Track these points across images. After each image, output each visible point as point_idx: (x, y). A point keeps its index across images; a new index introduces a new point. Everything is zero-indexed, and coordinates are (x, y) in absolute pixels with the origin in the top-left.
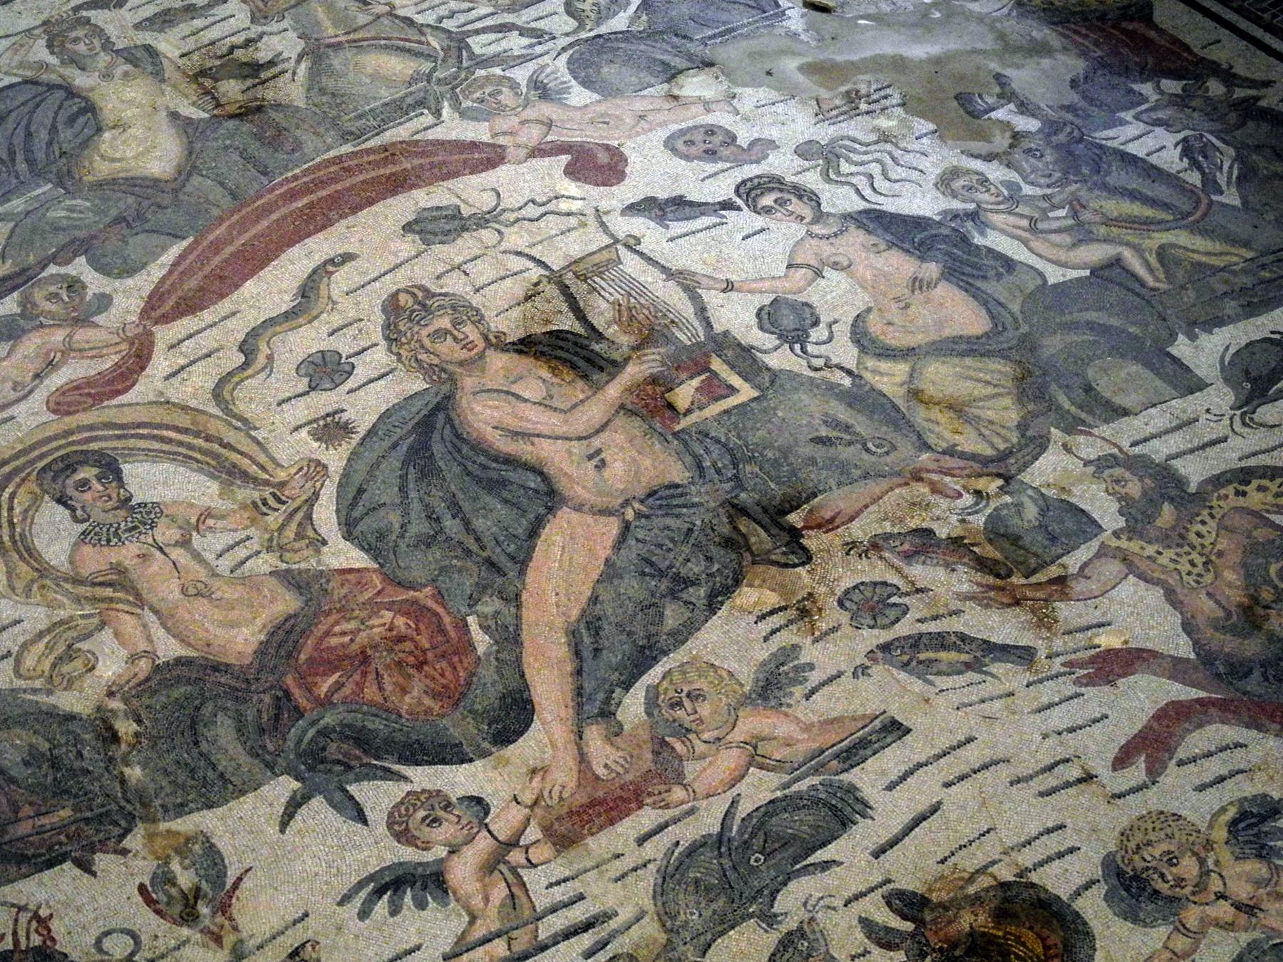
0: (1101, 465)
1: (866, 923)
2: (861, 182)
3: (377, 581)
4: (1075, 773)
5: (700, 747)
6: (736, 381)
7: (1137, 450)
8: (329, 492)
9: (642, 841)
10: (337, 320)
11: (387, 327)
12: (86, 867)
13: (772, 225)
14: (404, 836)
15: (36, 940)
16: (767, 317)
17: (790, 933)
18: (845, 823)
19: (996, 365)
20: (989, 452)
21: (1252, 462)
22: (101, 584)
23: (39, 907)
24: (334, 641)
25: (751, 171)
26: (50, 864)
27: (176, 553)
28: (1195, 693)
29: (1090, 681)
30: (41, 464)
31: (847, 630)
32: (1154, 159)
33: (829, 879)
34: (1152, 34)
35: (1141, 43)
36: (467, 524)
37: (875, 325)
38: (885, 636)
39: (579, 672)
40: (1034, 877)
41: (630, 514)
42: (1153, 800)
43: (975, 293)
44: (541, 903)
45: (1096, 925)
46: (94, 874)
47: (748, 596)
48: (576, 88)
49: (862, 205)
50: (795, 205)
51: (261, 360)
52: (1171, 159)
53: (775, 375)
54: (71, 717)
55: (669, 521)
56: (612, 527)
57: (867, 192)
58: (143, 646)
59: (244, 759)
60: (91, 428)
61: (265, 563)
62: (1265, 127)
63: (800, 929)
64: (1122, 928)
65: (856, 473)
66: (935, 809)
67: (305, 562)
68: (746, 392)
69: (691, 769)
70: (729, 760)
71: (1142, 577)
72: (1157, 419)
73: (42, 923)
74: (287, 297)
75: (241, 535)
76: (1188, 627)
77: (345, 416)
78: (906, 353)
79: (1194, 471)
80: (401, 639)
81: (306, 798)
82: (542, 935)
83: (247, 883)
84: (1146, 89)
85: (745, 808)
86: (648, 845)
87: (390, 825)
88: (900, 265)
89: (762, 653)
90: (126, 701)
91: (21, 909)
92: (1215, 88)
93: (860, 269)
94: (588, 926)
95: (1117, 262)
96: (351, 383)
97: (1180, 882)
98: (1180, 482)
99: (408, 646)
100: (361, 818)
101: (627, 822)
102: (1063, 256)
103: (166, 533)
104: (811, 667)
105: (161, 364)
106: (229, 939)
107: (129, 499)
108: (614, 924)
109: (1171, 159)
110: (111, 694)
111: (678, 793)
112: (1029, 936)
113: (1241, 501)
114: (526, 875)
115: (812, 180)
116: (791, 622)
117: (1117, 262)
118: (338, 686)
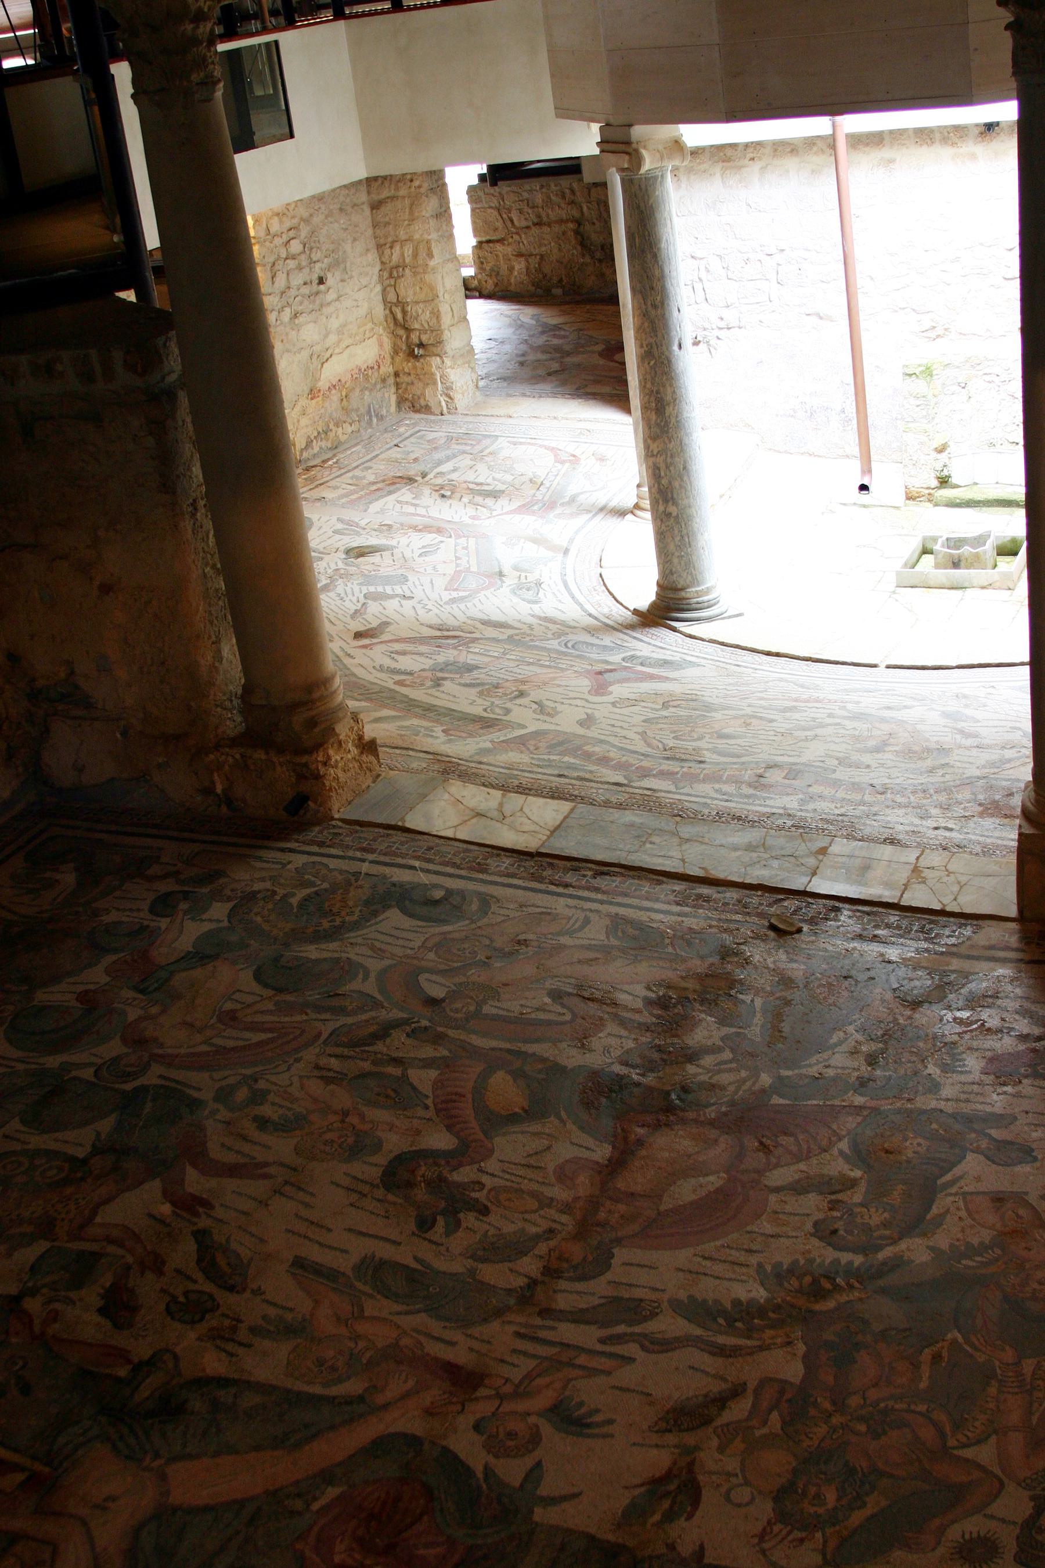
9: (452, 1344)
12: (700, 1553)
14: (535, 1439)
17: (475, 1260)
18: (383, 1264)
23: (754, 1546)
63: (471, 1257)
85: (397, 1307)
91: (763, 1552)
100: (539, 1464)
104: (264, 1317)
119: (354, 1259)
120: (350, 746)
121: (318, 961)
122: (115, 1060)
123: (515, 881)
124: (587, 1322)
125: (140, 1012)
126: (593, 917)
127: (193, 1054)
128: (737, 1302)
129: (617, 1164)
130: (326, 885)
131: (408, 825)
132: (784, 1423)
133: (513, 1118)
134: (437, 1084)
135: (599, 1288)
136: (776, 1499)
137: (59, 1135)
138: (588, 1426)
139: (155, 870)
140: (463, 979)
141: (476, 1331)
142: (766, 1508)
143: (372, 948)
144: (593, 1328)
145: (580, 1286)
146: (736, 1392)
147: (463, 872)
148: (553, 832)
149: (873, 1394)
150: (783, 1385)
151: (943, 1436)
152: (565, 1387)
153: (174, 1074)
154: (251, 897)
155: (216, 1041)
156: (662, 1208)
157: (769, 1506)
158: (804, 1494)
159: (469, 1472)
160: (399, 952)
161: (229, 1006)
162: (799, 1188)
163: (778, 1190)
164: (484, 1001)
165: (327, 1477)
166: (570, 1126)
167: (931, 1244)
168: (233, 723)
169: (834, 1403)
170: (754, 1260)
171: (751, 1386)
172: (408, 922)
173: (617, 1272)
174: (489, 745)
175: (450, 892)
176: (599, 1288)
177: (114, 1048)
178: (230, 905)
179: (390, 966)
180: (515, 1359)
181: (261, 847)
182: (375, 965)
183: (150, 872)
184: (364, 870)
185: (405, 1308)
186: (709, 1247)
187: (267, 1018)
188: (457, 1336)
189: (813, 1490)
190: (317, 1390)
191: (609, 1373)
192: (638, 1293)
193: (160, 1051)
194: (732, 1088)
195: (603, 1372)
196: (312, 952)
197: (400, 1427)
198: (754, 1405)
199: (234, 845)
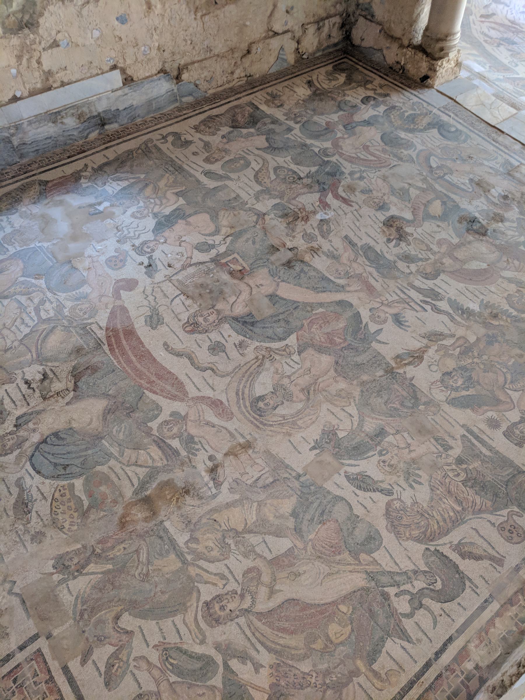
1: (394, 247)
3: (300, 333)
8: (267, 345)
9: (377, 281)
10: (195, 346)
11: (200, 333)
14: (385, 321)
18: (370, 248)
22: (309, 393)
26: (414, 386)
27: (292, 378)
30: (258, 417)
31: (318, 242)
34: (55, 182)
46: (414, 377)
48: (81, 290)
51: (210, 365)
54: (362, 391)
59: (367, 353)
60: (239, 407)
61: (296, 357)
66: (366, 233)
70: (355, 265)
74: (182, 360)
75: (285, 365)
77: (237, 342)
81: (377, 340)
83: (407, 348)
91: (430, 388)
96: (224, 342)
100: (382, 329)
103: (286, 381)
104: (328, 250)
105: (208, 392)
107: (272, 392)
108: (400, 286)
110: (352, 384)
118: (338, 337)
119: (364, 242)
120: (452, 62)
121: (402, 139)
122: (327, 149)
123: (480, 134)
124: (420, 293)
125: (341, 135)
126: (500, 157)
127: (350, 156)
128: (468, 308)
129: (458, 246)
130: (419, 112)
131: (457, 100)
132: (460, 353)
133: (434, 218)
134: (417, 197)
135: (430, 284)
136: (443, 375)
137: (299, 167)
138: (402, 325)
139: (369, 86)
140: (444, 163)
141: (386, 280)
142: (438, 376)
143: (422, 141)
144: (421, 295)
145: (425, 280)
146: (453, 336)
147: (465, 124)
148: (504, 120)
149: (492, 358)
150: (467, 341)
151: (506, 383)
152: (402, 310)
153: (341, 160)
154: (393, 107)
155: (359, 154)
156: (464, 267)
157: (440, 375)
158: (453, 378)
159: (361, 322)
160: (429, 145)
161: (368, 144)
162: (510, 280)
163: (504, 278)
164: (447, 174)
165: (321, 305)
166: (450, 227)
168: (418, 38)
169: (478, 355)
170: (482, 297)
172: (438, 136)
173: (437, 281)
174: (502, 77)
175: (457, 130)
176: (430, 284)
177: (328, 145)
178: (386, 108)
179: (424, 150)
180: (393, 294)
181: (406, 90)
182: (420, 147)
183: (368, 86)
184: (434, 111)
185: (369, 264)
186: (471, 287)
187: (378, 153)
188: (380, 280)
189: (456, 378)
190: (332, 278)
191: (417, 312)
192: (440, 291)
193: (340, 151)
194: (509, 237)
195: (416, 310)
196: (402, 135)
197: (349, 300)
198: (454, 343)
199: (398, 86)
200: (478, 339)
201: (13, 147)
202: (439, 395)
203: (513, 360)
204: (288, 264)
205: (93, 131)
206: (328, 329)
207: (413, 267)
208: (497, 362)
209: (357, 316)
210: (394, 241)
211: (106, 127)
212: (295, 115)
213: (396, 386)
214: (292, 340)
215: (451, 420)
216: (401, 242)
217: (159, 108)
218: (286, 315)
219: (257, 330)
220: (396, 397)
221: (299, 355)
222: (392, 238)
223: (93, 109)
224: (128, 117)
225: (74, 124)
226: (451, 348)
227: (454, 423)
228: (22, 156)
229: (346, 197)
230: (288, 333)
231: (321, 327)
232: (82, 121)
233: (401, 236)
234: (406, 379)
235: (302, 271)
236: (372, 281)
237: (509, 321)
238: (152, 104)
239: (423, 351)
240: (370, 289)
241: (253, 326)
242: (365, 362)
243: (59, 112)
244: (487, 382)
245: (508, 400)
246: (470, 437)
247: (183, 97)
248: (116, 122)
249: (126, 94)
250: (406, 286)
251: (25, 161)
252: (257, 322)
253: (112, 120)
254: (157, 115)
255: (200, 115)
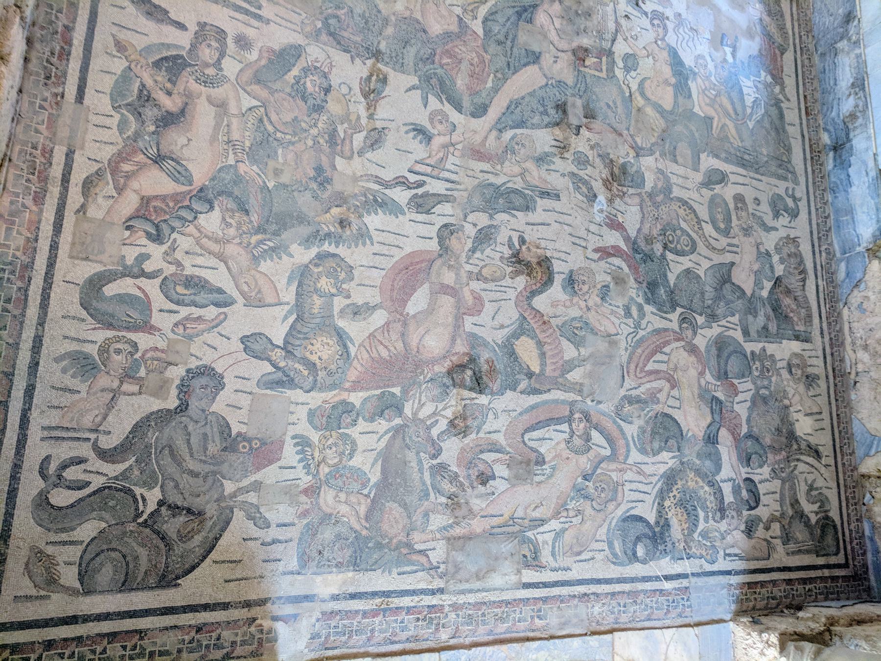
0: (661, 171)
1: (510, 237)
2: (681, 38)
3: (480, 42)
4: (584, 244)
5: (514, 160)
6: (604, 68)
7: (670, 175)
13: (651, 31)
14: (431, 120)
15: (326, 70)
16: (627, 57)
19: (662, 121)
20: (640, 145)
21: (689, 201)
24: (457, 50)
25: (660, 9)
26: (345, 51)
28: (625, 248)
29: (607, 225)
31: (570, 162)
32: (746, 97)
33: (513, 220)
34: (779, 59)
35: (774, 59)
36: (512, 47)
37: (647, 84)
38: (576, 171)
39: (504, 114)
40: (553, 261)
41: (550, 83)
42: (593, 265)
43: (676, 96)
44: (448, 166)
45: (555, 283)
47: (557, 131)
49: (675, 46)
50: (660, 30)
52: (749, 101)
53: (614, 76)
54: (379, 11)
55: (557, 93)
56: (543, 82)
57: (679, 43)
58: (412, 7)
59: (411, 64)
61: (458, 11)
62: (777, 112)
64: (560, 288)
65: (608, 121)
66: (548, 225)
67: (467, 19)
68: (603, 75)
69: (507, 163)
70: (517, 169)
71: (641, 208)
72: (681, 170)
73: (331, 66)
76: (639, 230)
78: (647, 99)
79: (676, 192)
80: (472, 64)
81: (417, 88)
82: (441, 175)
83: (386, 99)
84: (763, 74)
85: (510, 185)
86: (481, 174)
87: (431, 114)
88: (667, 71)
89: (547, 149)
90: (396, 20)
91: (329, 57)
92: (777, 89)
93: (658, 64)
94: (453, 182)
95: (711, 119)
97: (581, 290)
98: (671, 192)
99: (472, 68)
101: (482, 164)
102: (703, 104)
104: (554, 163)
106: (371, 111)
108: (458, 187)
109: (749, 101)
111: (499, 167)
112: (540, 274)
113: (678, 209)
114: (450, 156)
115: (670, 25)
116: (559, 147)
117: (711, 119)
118: (448, 64)
136: (331, 86)
165: (496, 90)
167: (292, 259)
171: (356, 155)
173: (433, 231)
186: (398, 255)
189: (317, 89)
200: (334, 167)
201: (836, 43)
202: (315, 53)
203: (280, 160)
204: (562, 108)
205: (830, 136)
206: (464, 66)
207: (470, 231)
208: (293, 143)
209: (459, 108)
210: (518, 247)
211: (831, 154)
212: (768, 371)
213: (358, 39)
214: (477, 27)
215: (283, 23)
216: (511, 252)
217: (839, 227)
218: (508, 49)
219: (511, 12)
220: (348, 24)
221: (458, 16)
222: (524, 248)
223: (858, 131)
224: (839, 182)
225: (845, 111)
226: (350, 131)
227: (278, 20)
228: (823, 55)
229: (610, 260)
230: (487, 32)
231: (472, 64)
232: (846, 120)
233: (519, 262)
234: (358, 55)
235: (545, 113)
236: (486, 166)
237: (323, 226)
238: (847, 215)
239: (371, 107)
240: (479, 154)
241: (517, 12)
242: (405, 51)
243: (863, 89)
244: (285, 104)
245: (248, 89)
246: (253, 9)
247: (848, 262)
248: (835, 166)
249: (867, 174)
250: (455, 193)
251: (816, 59)
252: (519, 20)
253: (838, 161)
254: (831, 222)
255: (812, 265)
